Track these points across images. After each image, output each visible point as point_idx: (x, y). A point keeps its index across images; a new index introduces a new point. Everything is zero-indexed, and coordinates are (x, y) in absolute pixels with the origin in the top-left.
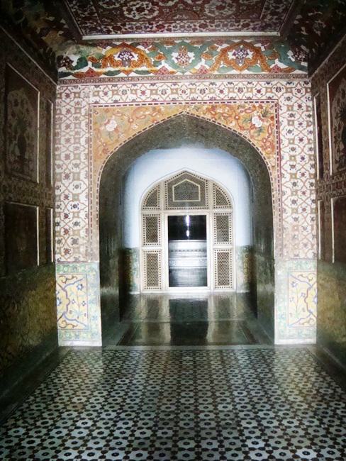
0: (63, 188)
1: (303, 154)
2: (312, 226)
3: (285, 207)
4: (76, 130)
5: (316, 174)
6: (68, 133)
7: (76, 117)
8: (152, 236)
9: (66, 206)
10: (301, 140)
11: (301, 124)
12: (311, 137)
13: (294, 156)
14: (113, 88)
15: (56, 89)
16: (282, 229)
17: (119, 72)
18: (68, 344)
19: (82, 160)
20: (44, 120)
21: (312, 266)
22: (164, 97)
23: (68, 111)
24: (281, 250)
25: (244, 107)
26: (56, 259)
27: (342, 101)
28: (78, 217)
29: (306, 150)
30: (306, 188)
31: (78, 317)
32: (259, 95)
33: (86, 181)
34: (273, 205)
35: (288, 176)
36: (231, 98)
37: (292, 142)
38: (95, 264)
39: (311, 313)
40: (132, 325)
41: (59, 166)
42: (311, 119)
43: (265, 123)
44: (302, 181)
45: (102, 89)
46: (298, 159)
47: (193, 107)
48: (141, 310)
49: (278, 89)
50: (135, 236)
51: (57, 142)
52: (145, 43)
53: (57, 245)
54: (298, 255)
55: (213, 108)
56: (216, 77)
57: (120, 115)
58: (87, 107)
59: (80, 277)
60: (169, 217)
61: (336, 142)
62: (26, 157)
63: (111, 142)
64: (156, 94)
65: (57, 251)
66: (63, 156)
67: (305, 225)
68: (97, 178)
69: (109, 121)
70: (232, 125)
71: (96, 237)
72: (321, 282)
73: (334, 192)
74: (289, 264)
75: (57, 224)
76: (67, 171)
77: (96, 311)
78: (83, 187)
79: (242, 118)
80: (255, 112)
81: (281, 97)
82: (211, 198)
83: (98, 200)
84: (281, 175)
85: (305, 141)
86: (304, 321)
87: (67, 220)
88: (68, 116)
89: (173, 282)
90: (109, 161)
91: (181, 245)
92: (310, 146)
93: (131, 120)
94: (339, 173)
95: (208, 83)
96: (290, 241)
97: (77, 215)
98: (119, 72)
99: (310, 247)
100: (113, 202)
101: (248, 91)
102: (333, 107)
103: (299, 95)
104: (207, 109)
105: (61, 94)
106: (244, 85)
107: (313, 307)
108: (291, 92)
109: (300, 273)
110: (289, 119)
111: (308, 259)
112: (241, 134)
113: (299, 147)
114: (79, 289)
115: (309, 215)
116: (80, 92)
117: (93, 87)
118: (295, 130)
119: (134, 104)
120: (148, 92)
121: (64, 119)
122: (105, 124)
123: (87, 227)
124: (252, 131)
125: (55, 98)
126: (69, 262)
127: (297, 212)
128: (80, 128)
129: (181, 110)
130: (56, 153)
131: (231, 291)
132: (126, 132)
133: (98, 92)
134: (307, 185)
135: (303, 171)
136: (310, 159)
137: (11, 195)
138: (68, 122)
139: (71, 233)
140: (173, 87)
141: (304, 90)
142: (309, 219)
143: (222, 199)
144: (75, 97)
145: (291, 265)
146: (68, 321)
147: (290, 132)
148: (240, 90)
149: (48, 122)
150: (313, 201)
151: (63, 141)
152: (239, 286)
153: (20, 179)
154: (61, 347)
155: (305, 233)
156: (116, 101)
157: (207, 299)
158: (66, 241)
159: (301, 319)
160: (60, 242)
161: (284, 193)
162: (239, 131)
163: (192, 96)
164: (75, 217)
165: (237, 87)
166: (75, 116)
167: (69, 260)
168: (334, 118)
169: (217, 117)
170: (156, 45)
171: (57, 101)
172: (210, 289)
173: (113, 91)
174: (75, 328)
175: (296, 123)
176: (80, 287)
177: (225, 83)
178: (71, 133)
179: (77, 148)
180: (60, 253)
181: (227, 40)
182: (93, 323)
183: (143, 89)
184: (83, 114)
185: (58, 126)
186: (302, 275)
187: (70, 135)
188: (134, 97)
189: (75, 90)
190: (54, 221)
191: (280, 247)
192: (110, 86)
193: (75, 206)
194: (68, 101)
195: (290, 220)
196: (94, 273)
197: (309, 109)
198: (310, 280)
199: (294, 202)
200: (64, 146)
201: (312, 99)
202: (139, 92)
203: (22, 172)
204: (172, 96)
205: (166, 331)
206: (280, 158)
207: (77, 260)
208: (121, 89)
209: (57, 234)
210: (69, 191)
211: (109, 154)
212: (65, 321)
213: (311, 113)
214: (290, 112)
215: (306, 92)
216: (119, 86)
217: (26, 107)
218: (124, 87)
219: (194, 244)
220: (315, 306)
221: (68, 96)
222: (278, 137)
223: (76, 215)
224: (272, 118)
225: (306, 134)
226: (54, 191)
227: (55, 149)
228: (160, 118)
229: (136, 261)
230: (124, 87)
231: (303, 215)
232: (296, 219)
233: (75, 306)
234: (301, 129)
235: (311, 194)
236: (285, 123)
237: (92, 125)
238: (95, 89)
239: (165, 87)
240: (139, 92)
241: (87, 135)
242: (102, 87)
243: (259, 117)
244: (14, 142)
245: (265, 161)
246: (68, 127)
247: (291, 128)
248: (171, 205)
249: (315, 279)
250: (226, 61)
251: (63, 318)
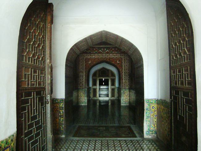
8: (94, 84)
10: (126, 66)
11: (126, 63)
16: (122, 83)
17: (91, 52)
18: (81, 105)
48: (92, 102)
49: (122, 56)
52: (97, 47)
55: (110, 59)
56: (111, 53)
74: (124, 90)
75: (79, 81)
82: (110, 75)
84: (122, 73)
91: (102, 87)
97: (83, 80)
98: (91, 52)
107: (128, 98)
120: (97, 56)
143: (113, 75)
147: (124, 64)
148: (115, 56)
170: (99, 48)
181: (112, 47)
195: (124, 81)
199: (125, 78)
206: (122, 69)
219: (105, 87)
221: (81, 56)
228: (99, 61)
232: (125, 81)
246: (81, 62)
248: (100, 76)
250: (112, 50)
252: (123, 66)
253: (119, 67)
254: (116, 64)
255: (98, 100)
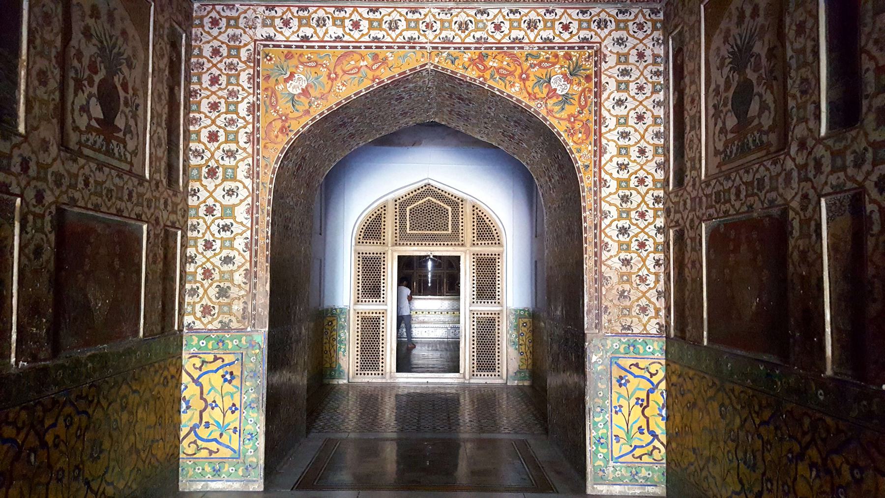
0: (203, 194)
1: (643, 144)
2: (657, 275)
3: (606, 240)
4: (230, 88)
5: (667, 180)
6: (214, 93)
7: (231, 64)
8: (371, 288)
9: (208, 228)
10: (640, 118)
11: (641, 88)
12: (660, 112)
13: (626, 148)
14: (301, 13)
15: (192, 9)
16: (600, 279)
18: (199, 486)
19: (242, 144)
20: (164, 63)
21: (657, 347)
22: (394, 35)
23: (216, 52)
24: (598, 316)
25: (537, 57)
26: (185, 324)
27: (735, 31)
28: (232, 247)
29: (648, 136)
30: (647, 205)
31: (221, 435)
32: (566, 35)
33: (248, 182)
34: (584, 235)
35: (613, 185)
36: (516, 40)
37: (622, 121)
38: (261, 336)
39: (655, 436)
40: (329, 443)
41: (198, 154)
42: (661, 80)
43: (575, 88)
44: (639, 193)
45: (280, 14)
46: (634, 152)
47: (445, 55)
50: (344, 290)
51: (194, 107)
53: (187, 299)
54: (629, 328)
55: (482, 57)
57: (314, 64)
58: (251, 47)
59: (229, 359)
60: (399, 257)
61: (716, 116)
62: (120, 122)
63: (296, 114)
64: (380, 28)
65: (189, 309)
66: (204, 134)
67: (644, 272)
68: (268, 178)
69: (292, 75)
70: (515, 91)
71: (264, 286)
72: (674, 379)
73: (712, 211)
74: (613, 344)
76: (212, 164)
77: (256, 422)
78: (243, 193)
79: (532, 77)
80: (558, 66)
81: (607, 39)
83: (270, 219)
84: (601, 183)
85: (649, 120)
86: (644, 451)
87: (209, 253)
88: (215, 61)
89: (404, 363)
90: (292, 148)
91: (423, 303)
92: (656, 129)
93: (333, 76)
94: (721, 173)
95: (473, 12)
96: (616, 302)
99: (652, 312)
100: (302, 224)
101: (546, 27)
102: (713, 46)
103: (641, 35)
104: (470, 59)
105: (201, 18)
106: (538, 14)
107: (660, 426)
108: (626, 28)
109: (634, 361)
110: (620, 78)
111: (648, 335)
112: (530, 108)
113: (636, 130)
114: (225, 380)
115: (652, 255)
116: (239, 17)
117: (261, 9)
118: (630, 99)
119: (339, 44)
120: (364, 24)
121: (207, 65)
122: (286, 81)
123: (247, 266)
124: (550, 102)
125: (192, 25)
126: (211, 330)
127: (628, 249)
128: (238, 85)
129: (423, 61)
130: (191, 128)
131: (498, 381)
132: (323, 97)
133: (273, 18)
134: (649, 200)
135: (641, 174)
136: (656, 153)
137: (77, 195)
138: (215, 72)
139: (216, 276)
140: (410, 16)
141: (650, 24)
142: (650, 263)
144: (228, 26)
145: (616, 345)
146: (199, 442)
147: (620, 102)
149: (174, 67)
150: (659, 230)
151: (204, 107)
152: (511, 373)
153: (121, 173)
154: (184, 493)
155: (643, 288)
156: (305, 39)
157: (458, 395)
158: (206, 291)
159: (636, 447)
160: (194, 292)
161: (605, 215)
162: (526, 101)
163: (443, 34)
164: (228, 248)
165: (527, 18)
166: (228, 61)
167: (210, 327)
168: (713, 69)
169: (487, 75)
171: (194, 31)
172: (464, 377)
173: (300, 19)
174: (214, 455)
175: (633, 87)
176: (228, 377)
177: (505, 11)
178: (220, 93)
179: (232, 122)
180: (194, 314)
182: (249, 445)
183: (356, 17)
184: (244, 59)
185: (195, 79)
186: (637, 365)
187: (220, 98)
188: (340, 32)
189: (228, 13)
190: (183, 254)
191: (595, 312)
192: (295, 10)
193: (226, 228)
194: (215, 32)
195: (616, 263)
196: (258, 351)
197: (659, 60)
198: (652, 375)
199: (623, 231)
200: (206, 116)
201: (665, 42)
202: (348, 23)
203: (109, 153)
204: (407, 34)
205: (390, 453)
206: (600, 151)
207: (225, 327)
208: (315, 16)
209: (190, 278)
210: (216, 201)
211: (291, 135)
212: (195, 442)
213: (662, 69)
214: (622, 67)
215: (655, 28)
216: (311, 10)
217: (119, 25)
218: (321, 13)
220: (663, 424)
221: (215, 23)
222: (598, 113)
223: (227, 244)
224: (588, 78)
225: (650, 107)
226: (186, 200)
227: (189, 122)
228: (385, 75)
229: (343, 328)
230: (321, 13)
231: (639, 256)
232: (626, 262)
233: (217, 414)
234: (640, 97)
235: (656, 216)
236: (612, 85)
237: (260, 80)
238: (267, 12)
239: (395, 16)
240: (348, 23)
241: (251, 99)
242: (280, 11)
243: (565, 75)
244: (88, 90)
245: (572, 156)
246: (214, 80)
247: (623, 96)
248: (403, 238)
249: (662, 374)
251: (192, 437)
252: (611, 122)
253: (571, 133)
254: (539, 108)
255: (392, 387)
